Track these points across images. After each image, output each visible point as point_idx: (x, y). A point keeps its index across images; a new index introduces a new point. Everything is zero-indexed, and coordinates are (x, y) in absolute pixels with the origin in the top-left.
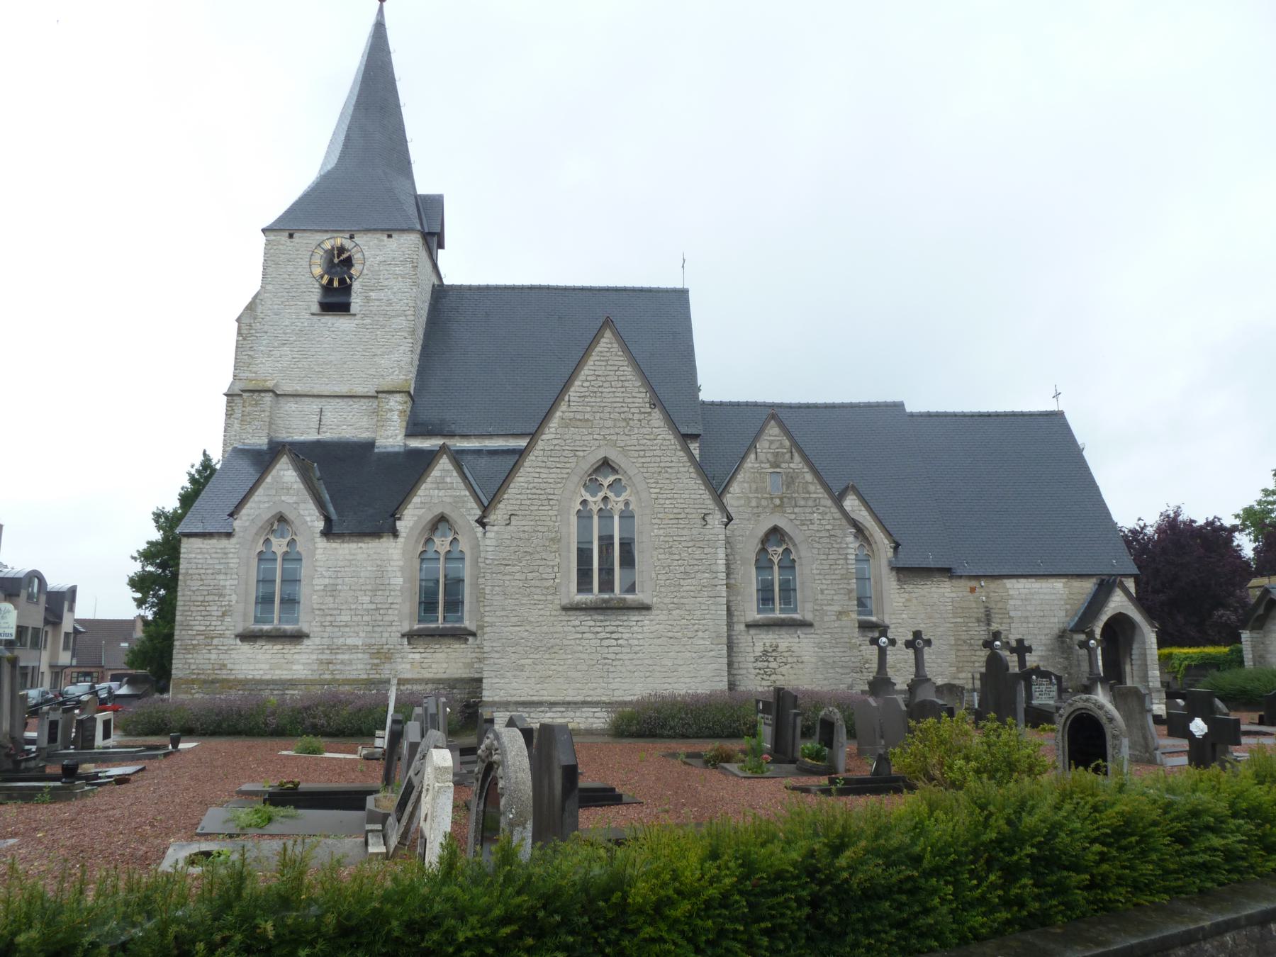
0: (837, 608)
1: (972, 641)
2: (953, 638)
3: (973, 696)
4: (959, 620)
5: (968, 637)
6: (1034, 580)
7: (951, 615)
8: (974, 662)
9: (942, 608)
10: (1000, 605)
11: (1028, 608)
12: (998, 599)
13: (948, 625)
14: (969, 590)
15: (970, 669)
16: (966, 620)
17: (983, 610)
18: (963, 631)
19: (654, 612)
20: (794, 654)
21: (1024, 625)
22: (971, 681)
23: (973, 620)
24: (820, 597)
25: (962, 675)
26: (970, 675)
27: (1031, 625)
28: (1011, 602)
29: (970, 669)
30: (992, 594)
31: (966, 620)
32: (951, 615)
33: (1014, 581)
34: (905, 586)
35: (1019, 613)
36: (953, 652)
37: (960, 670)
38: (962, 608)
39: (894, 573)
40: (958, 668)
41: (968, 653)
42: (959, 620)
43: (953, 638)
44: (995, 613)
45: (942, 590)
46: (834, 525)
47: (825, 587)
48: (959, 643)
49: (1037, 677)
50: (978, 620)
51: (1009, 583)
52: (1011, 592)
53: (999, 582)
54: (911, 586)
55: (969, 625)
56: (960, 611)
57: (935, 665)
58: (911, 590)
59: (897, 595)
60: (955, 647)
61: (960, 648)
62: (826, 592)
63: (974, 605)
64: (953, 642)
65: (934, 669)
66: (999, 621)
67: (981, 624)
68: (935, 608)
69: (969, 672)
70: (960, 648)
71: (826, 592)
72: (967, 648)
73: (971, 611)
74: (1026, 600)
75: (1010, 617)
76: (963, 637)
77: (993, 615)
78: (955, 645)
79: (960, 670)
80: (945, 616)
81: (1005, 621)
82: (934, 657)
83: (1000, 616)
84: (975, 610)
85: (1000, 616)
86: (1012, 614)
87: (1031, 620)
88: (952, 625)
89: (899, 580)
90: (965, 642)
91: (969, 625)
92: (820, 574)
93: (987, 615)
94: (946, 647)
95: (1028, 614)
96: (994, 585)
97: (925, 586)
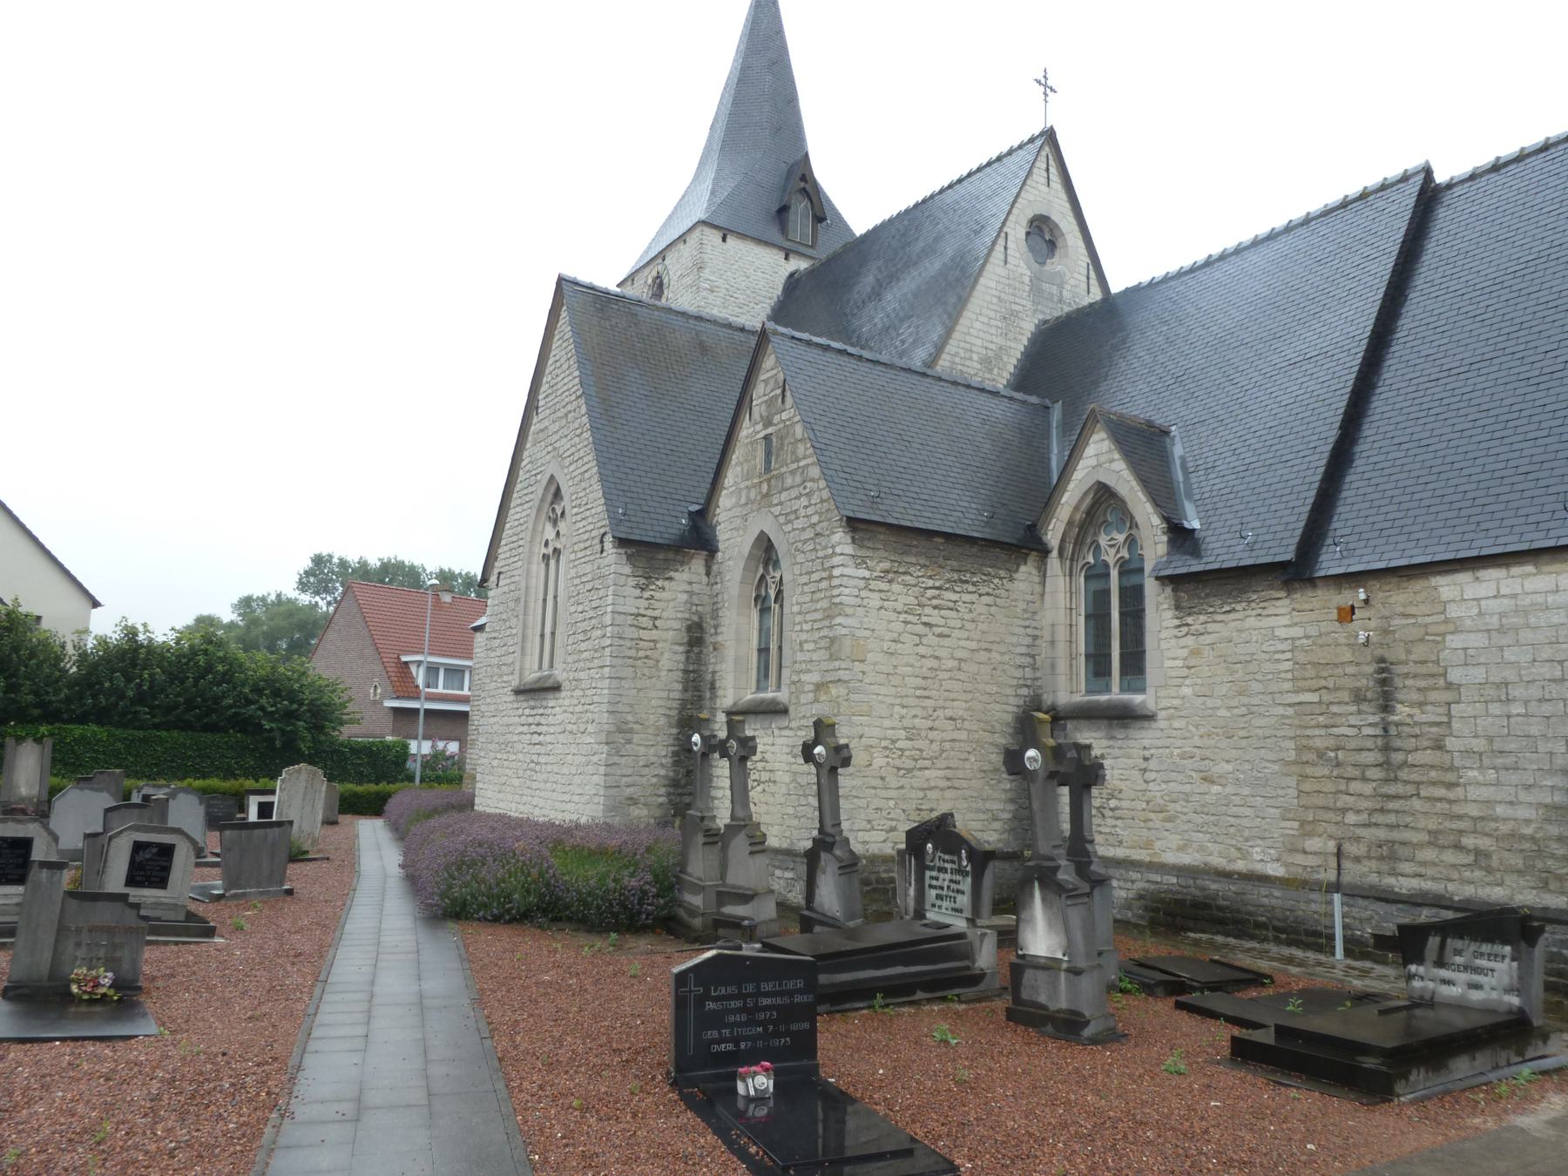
0: (815, 678)
1: (1340, 753)
2: (1291, 744)
3: (1330, 902)
4: (1314, 697)
5: (1331, 742)
6: (1530, 568)
7: (1287, 686)
8: (1344, 811)
9: (1268, 667)
10: (1419, 652)
11: (1509, 655)
12: (1415, 633)
13: (1280, 711)
14: (1335, 615)
15: (1332, 829)
16: (1327, 697)
17: (1370, 669)
18: (1318, 726)
19: (563, 694)
20: (769, 766)
21: (1495, 709)
22: (1333, 862)
23: (1345, 695)
24: (800, 656)
25: (1313, 844)
26: (1331, 846)
27: (1517, 709)
28: (1454, 641)
29: (1332, 829)
30: (1397, 622)
31: (1327, 697)
32: (1287, 686)
33: (1464, 577)
34: (1189, 620)
35: (1479, 674)
36: (1292, 781)
37: (1307, 827)
38: (1315, 664)
39: (1168, 590)
40: (1303, 823)
41: (1329, 787)
42: (1314, 697)
43: (1291, 744)
44: (1406, 675)
45: (1270, 622)
46: (820, 514)
47: (804, 636)
48: (1312, 756)
49: (935, 848)
50: (1358, 697)
51: (1447, 586)
52: (1454, 611)
53: (1418, 585)
54: (1202, 618)
55: (1334, 709)
56: (1311, 672)
57: (1248, 812)
58: (1201, 628)
59: (1173, 641)
60: (1294, 768)
61: (1309, 770)
62: (806, 646)
63: (1348, 656)
64: (1292, 755)
65: (1245, 822)
66: (1415, 696)
67: (1365, 707)
68: (1252, 667)
69: (1331, 837)
70: (1309, 770)
71: (806, 646)
72: (1326, 772)
73: (1339, 671)
74: (1501, 630)
75: (1449, 686)
76: (1318, 743)
77: (1398, 682)
78: (1295, 762)
79: (1307, 827)
80: (1274, 687)
81: (1434, 696)
82: (1246, 791)
83: (1422, 683)
84: (1350, 670)
85: (1422, 683)
86: (1455, 675)
87: (1516, 692)
88: (1290, 711)
89: (1178, 607)
90: (1321, 754)
91: (1334, 709)
92: (800, 613)
93: (1384, 682)
94: (1276, 768)
95: (1510, 674)
96: (1399, 597)
97: (1232, 616)
